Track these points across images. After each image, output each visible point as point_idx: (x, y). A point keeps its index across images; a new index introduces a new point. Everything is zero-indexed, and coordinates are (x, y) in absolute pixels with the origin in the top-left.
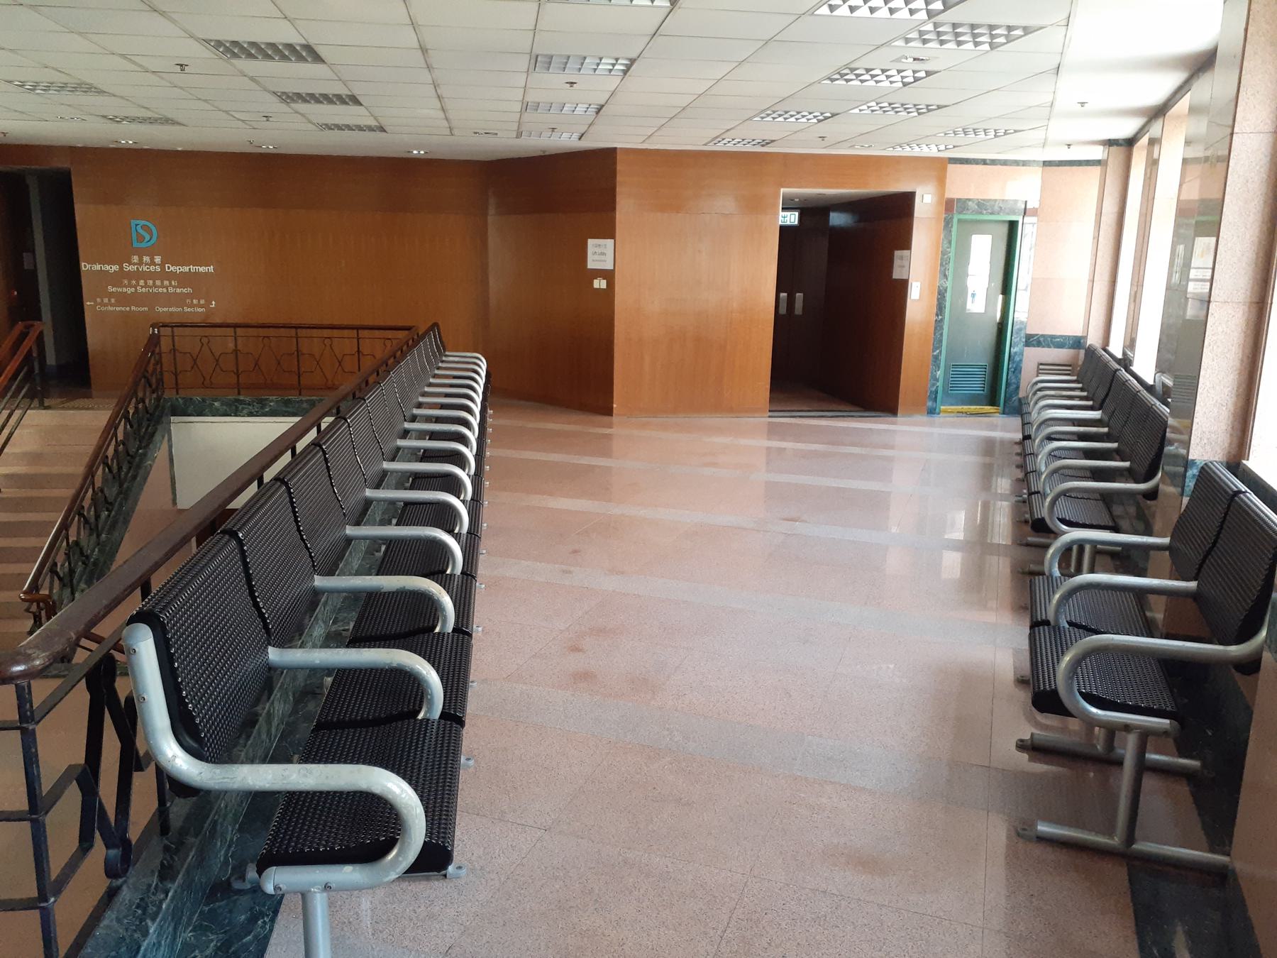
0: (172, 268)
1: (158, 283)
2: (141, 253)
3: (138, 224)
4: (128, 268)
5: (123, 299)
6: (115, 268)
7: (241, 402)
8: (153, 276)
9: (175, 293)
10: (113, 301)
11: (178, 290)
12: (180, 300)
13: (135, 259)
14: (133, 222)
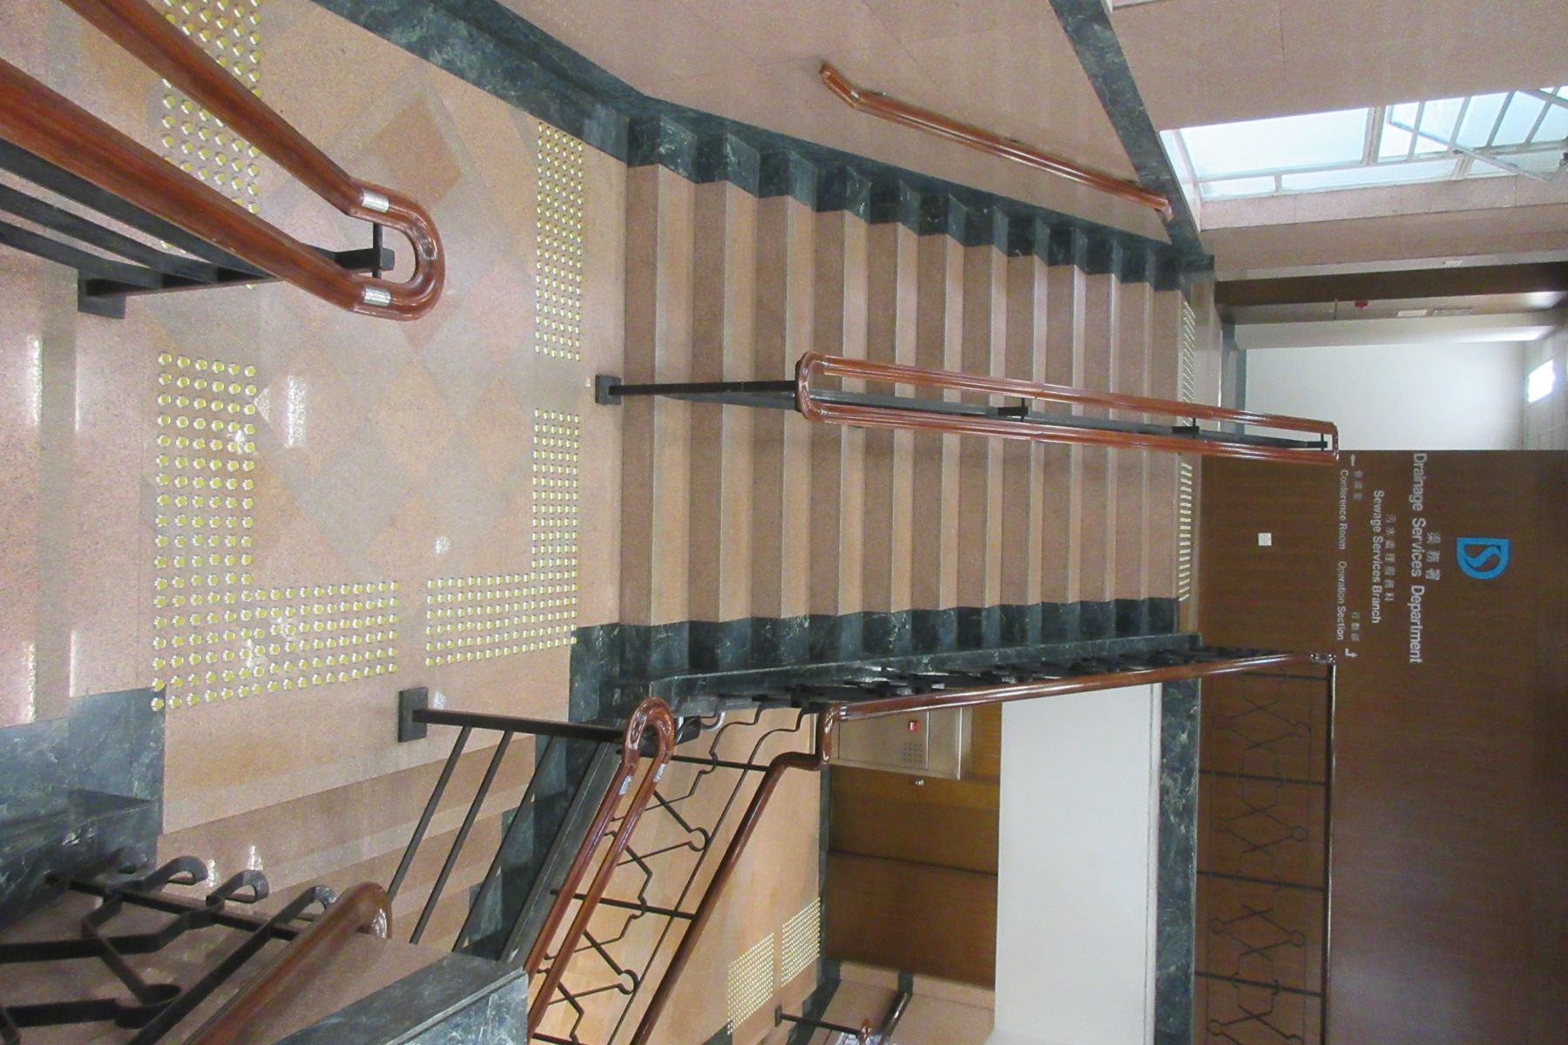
0: (1417, 595)
1: (1390, 571)
2: (1448, 549)
3: (1500, 548)
4: (1418, 526)
5: (1361, 513)
6: (1418, 505)
7: (1187, 780)
8: (1404, 562)
9: (1370, 596)
10: (1358, 496)
11: (1376, 603)
12: (1359, 597)
13: (1434, 538)
14: (1504, 543)
